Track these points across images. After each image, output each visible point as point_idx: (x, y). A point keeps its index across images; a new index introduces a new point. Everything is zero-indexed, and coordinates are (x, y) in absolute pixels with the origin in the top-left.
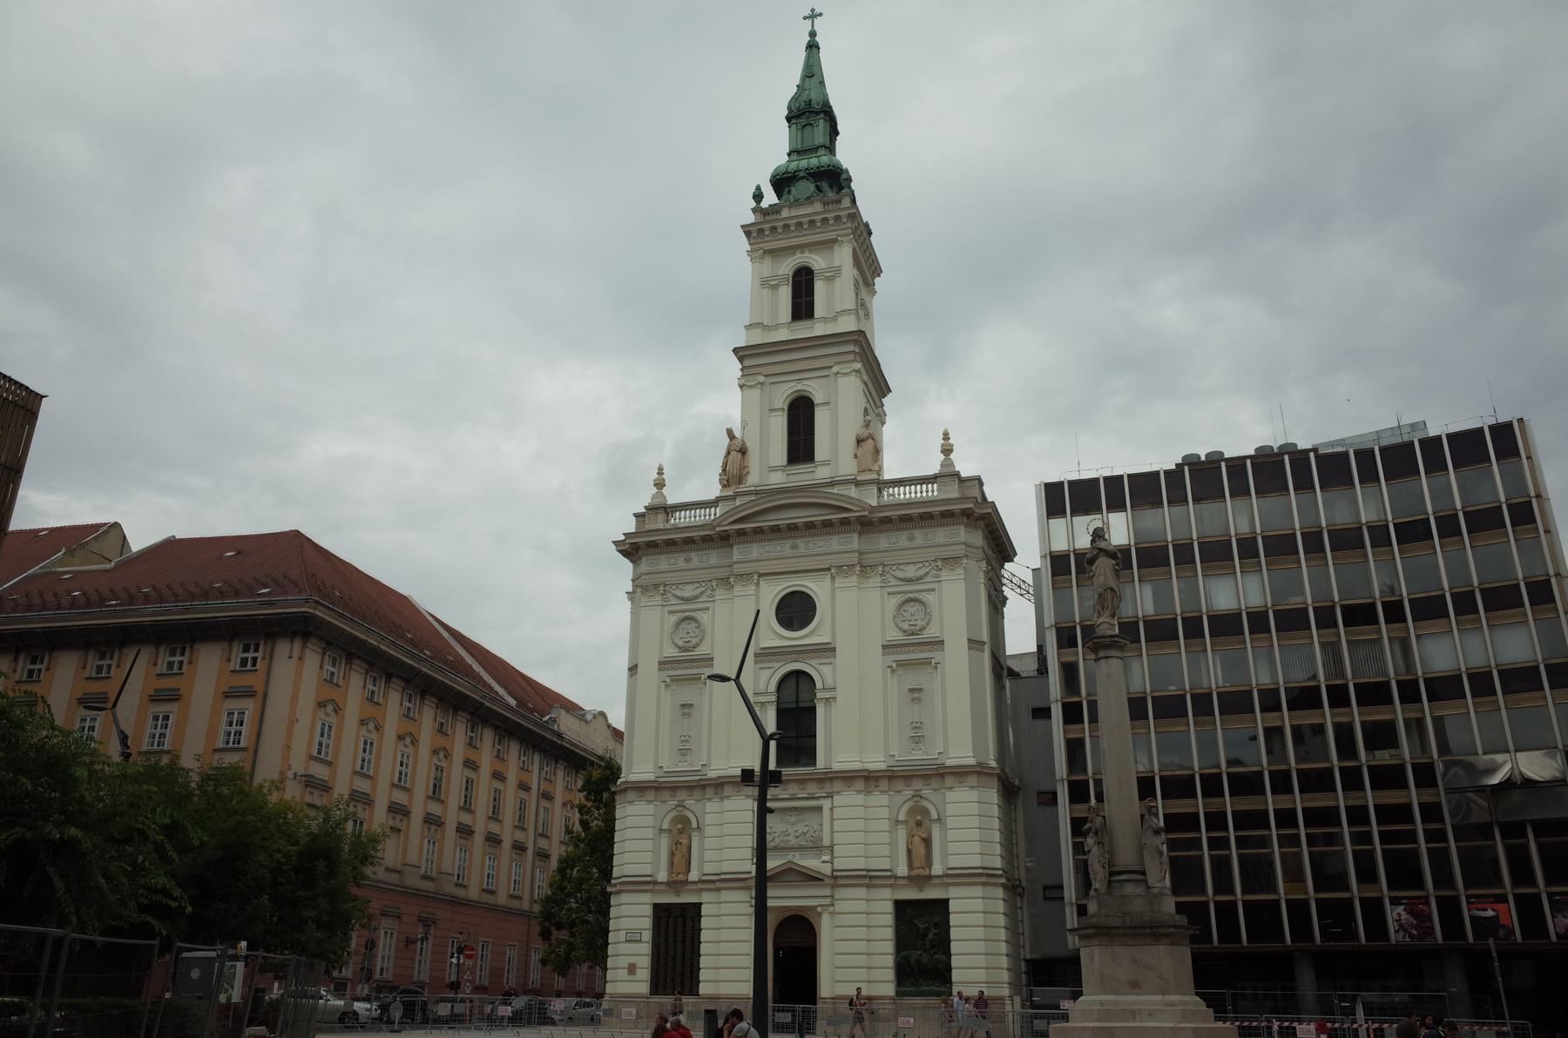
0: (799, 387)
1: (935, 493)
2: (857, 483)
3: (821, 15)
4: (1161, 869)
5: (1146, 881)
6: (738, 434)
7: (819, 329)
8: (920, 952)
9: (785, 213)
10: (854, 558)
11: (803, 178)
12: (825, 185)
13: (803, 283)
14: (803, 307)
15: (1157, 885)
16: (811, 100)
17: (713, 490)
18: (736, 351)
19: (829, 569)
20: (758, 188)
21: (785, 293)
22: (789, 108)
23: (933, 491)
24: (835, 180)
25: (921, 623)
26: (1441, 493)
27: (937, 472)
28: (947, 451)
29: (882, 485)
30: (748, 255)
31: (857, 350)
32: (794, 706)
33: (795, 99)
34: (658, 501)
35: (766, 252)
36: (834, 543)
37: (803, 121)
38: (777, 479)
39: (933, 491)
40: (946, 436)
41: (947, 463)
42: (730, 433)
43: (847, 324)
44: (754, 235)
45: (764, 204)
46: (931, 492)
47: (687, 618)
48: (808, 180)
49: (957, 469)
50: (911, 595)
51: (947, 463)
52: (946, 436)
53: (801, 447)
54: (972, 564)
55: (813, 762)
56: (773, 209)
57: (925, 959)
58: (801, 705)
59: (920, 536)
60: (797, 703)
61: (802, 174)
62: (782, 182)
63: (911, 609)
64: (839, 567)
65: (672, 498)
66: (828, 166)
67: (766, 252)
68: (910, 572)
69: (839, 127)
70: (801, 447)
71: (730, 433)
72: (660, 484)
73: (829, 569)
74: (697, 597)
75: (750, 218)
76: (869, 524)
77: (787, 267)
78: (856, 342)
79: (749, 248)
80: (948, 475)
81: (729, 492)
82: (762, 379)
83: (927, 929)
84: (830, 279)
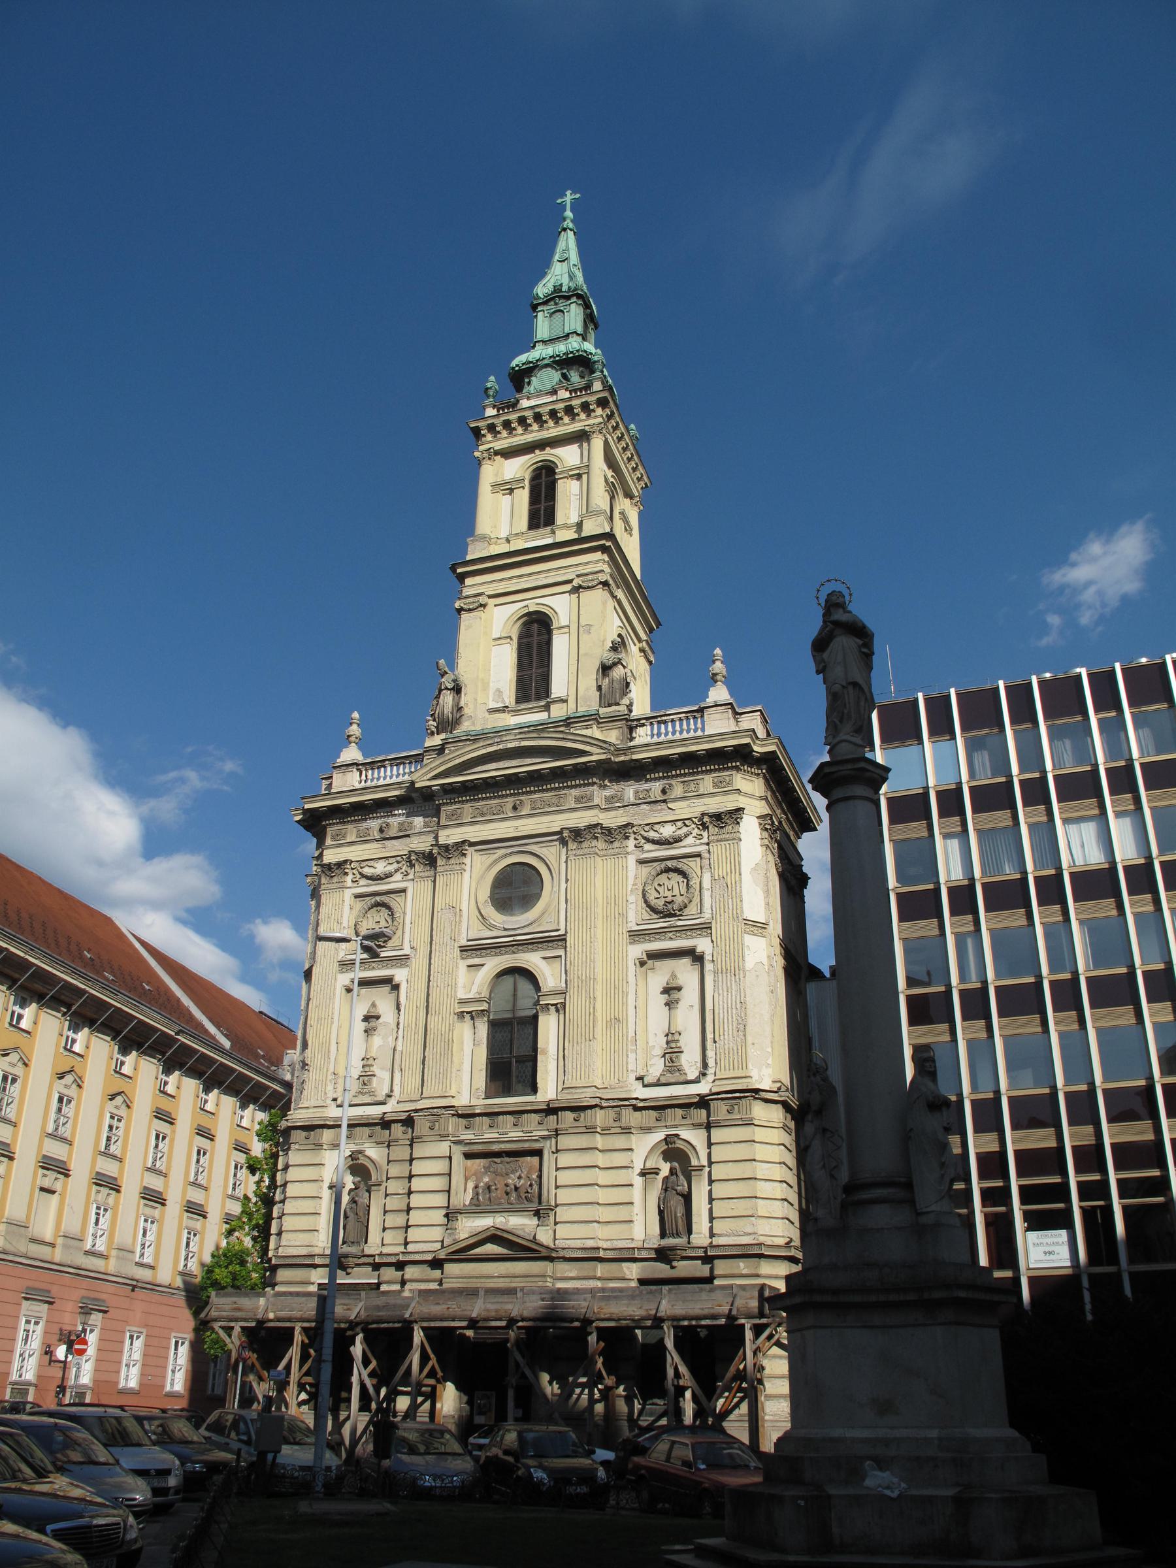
4: (943, 1176)
5: (912, 1202)
11: (546, 366)
15: (933, 1208)
16: (561, 285)
31: (607, 559)
32: (509, 1015)
47: (377, 904)
48: (553, 367)
50: (670, 864)
55: (534, 1090)
60: (513, 1011)
61: (546, 362)
66: (578, 351)
74: (389, 875)
78: (604, 549)
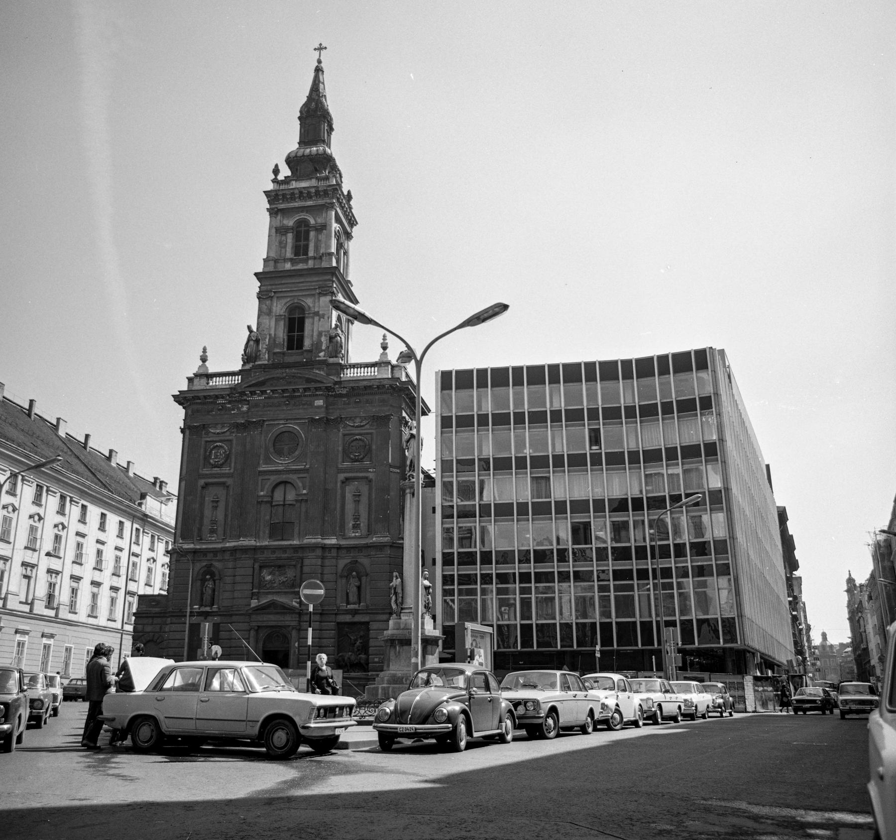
1: (376, 374)
3: (326, 48)
6: (254, 329)
7: (311, 264)
8: (350, 653)
14: (300, 250)
17: (237, 366)
18: (256, 274)
20: (277, 166)
22: (301, 112)
23: (374, 372)
26: (665, 391)
27: (377, 360)
29: (342, 367)
30: (268, 211)
31: (334, 279)
32: (282, 503)
33: (306, 105)
34: (201, 371)
39: (374, 372)
41: (384, 354)
42: (249, 328)
45: (281, 177)
49: (389, 359)
56: (287, 180)
57: (353, 658)
58: (287, 503)
65: (212, 368)
69: (334, 126)
71: (249, 328)
72: (204, 359)
75: (270, 187)
79: (268, 206)
81: (248, 367)
83: (356, 640)
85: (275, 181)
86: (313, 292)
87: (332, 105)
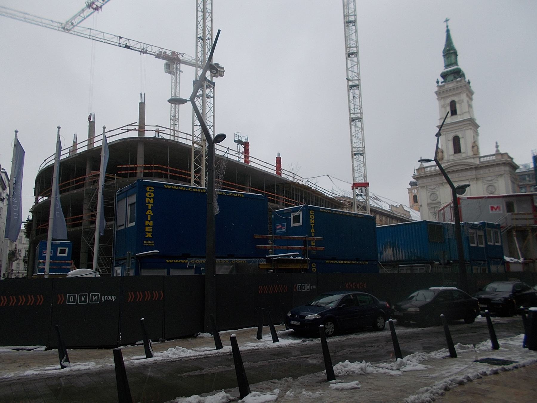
0: (455, 134)
2: (473, 158)
9: (446, 86)
10: (474, 177)
12: (456, 75)
13: (453, 105)
14: (454, 112)
19: (468, 180)
20: (438, 80)
21: (448, 109)
24: (458, 73)
25: (494, 191)
28: (497, 147)
29: (480, 157)
35: (442, 98)
36: (468, 173)
37: (447, 56)
38: (452, 158)
40: (497, 143)
41: (497, 151)
43: (467, 117)
44: (438, 94)
45: (440, 84)
46: (493, 158)
47: (433, 193)
51: (497, 151)
52: (497, 143)
53: (457, 149)
54: (506, 175)
59: (491, 170)
62: (444, 76)
63: (490, 187)
64: (471, 179)
67: (442, 98)
68: (490, 179)
70: (457, 149)
73: (468, 180)
74: (435, 188)
76: (477, 168)
77: (448, 101)
80: (498, 153)
82: (445, 133)
84: (460, 104)
85: (438, 86)
86: (462, 129)
87: (456, 44)
